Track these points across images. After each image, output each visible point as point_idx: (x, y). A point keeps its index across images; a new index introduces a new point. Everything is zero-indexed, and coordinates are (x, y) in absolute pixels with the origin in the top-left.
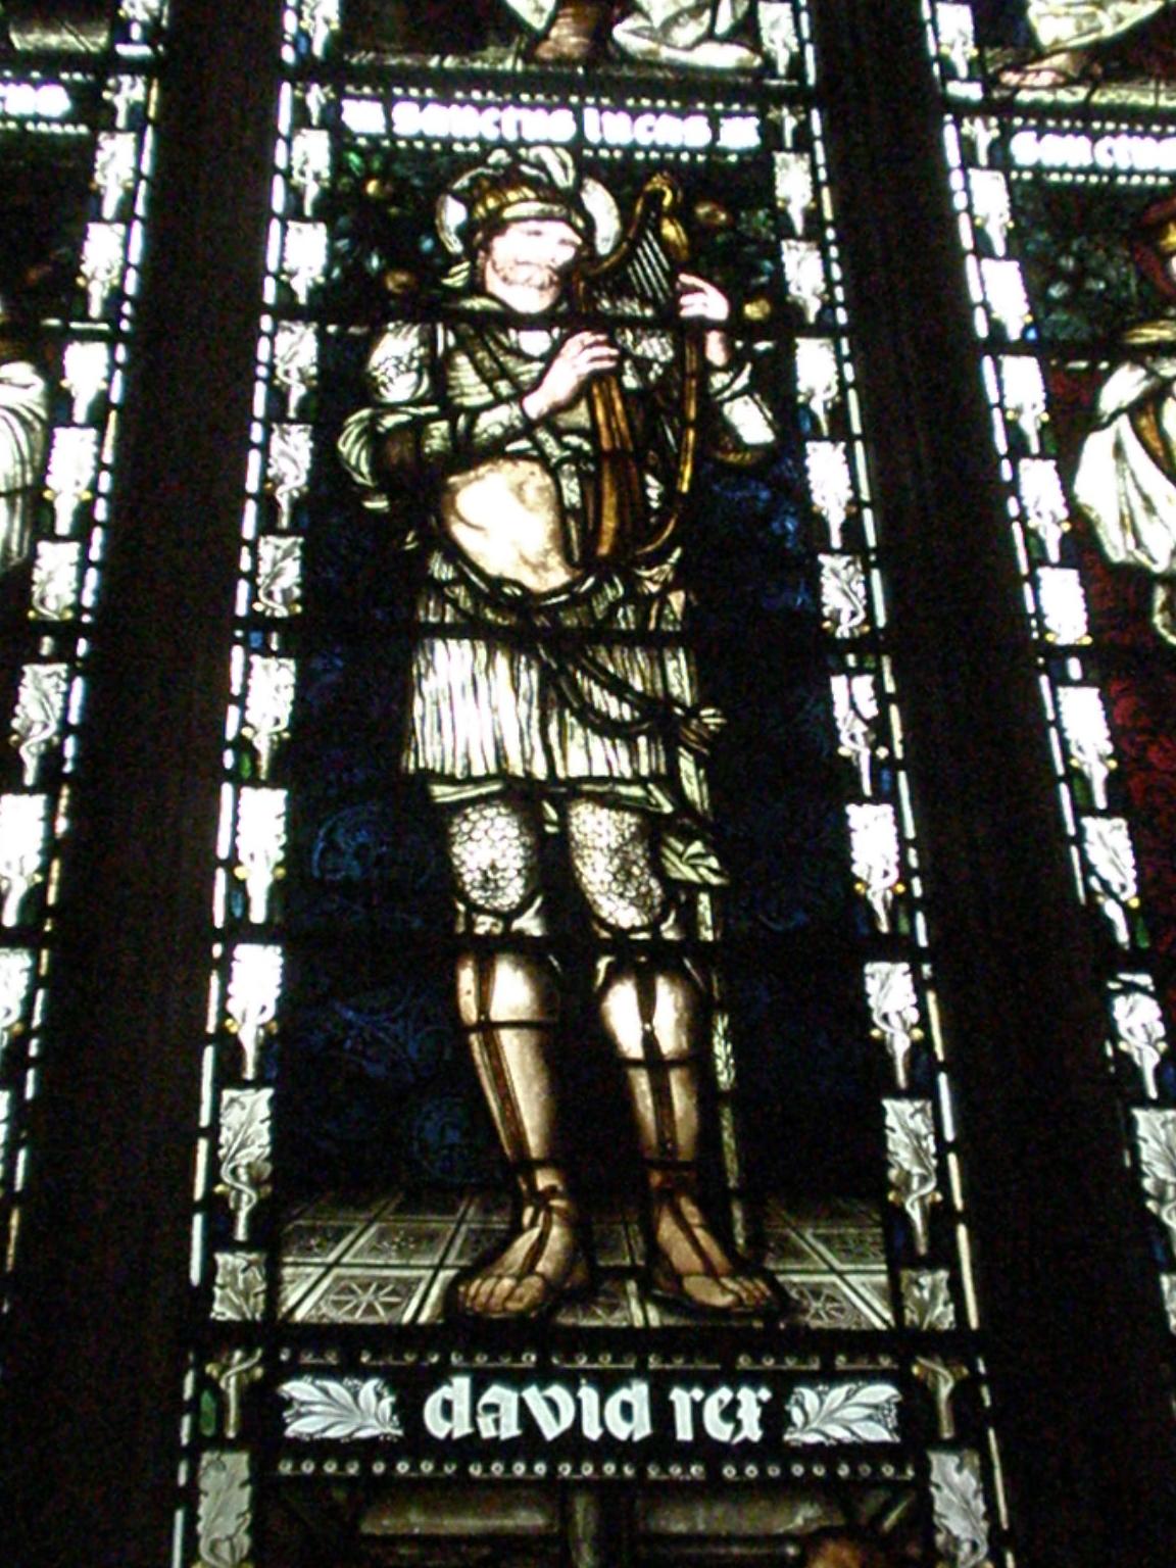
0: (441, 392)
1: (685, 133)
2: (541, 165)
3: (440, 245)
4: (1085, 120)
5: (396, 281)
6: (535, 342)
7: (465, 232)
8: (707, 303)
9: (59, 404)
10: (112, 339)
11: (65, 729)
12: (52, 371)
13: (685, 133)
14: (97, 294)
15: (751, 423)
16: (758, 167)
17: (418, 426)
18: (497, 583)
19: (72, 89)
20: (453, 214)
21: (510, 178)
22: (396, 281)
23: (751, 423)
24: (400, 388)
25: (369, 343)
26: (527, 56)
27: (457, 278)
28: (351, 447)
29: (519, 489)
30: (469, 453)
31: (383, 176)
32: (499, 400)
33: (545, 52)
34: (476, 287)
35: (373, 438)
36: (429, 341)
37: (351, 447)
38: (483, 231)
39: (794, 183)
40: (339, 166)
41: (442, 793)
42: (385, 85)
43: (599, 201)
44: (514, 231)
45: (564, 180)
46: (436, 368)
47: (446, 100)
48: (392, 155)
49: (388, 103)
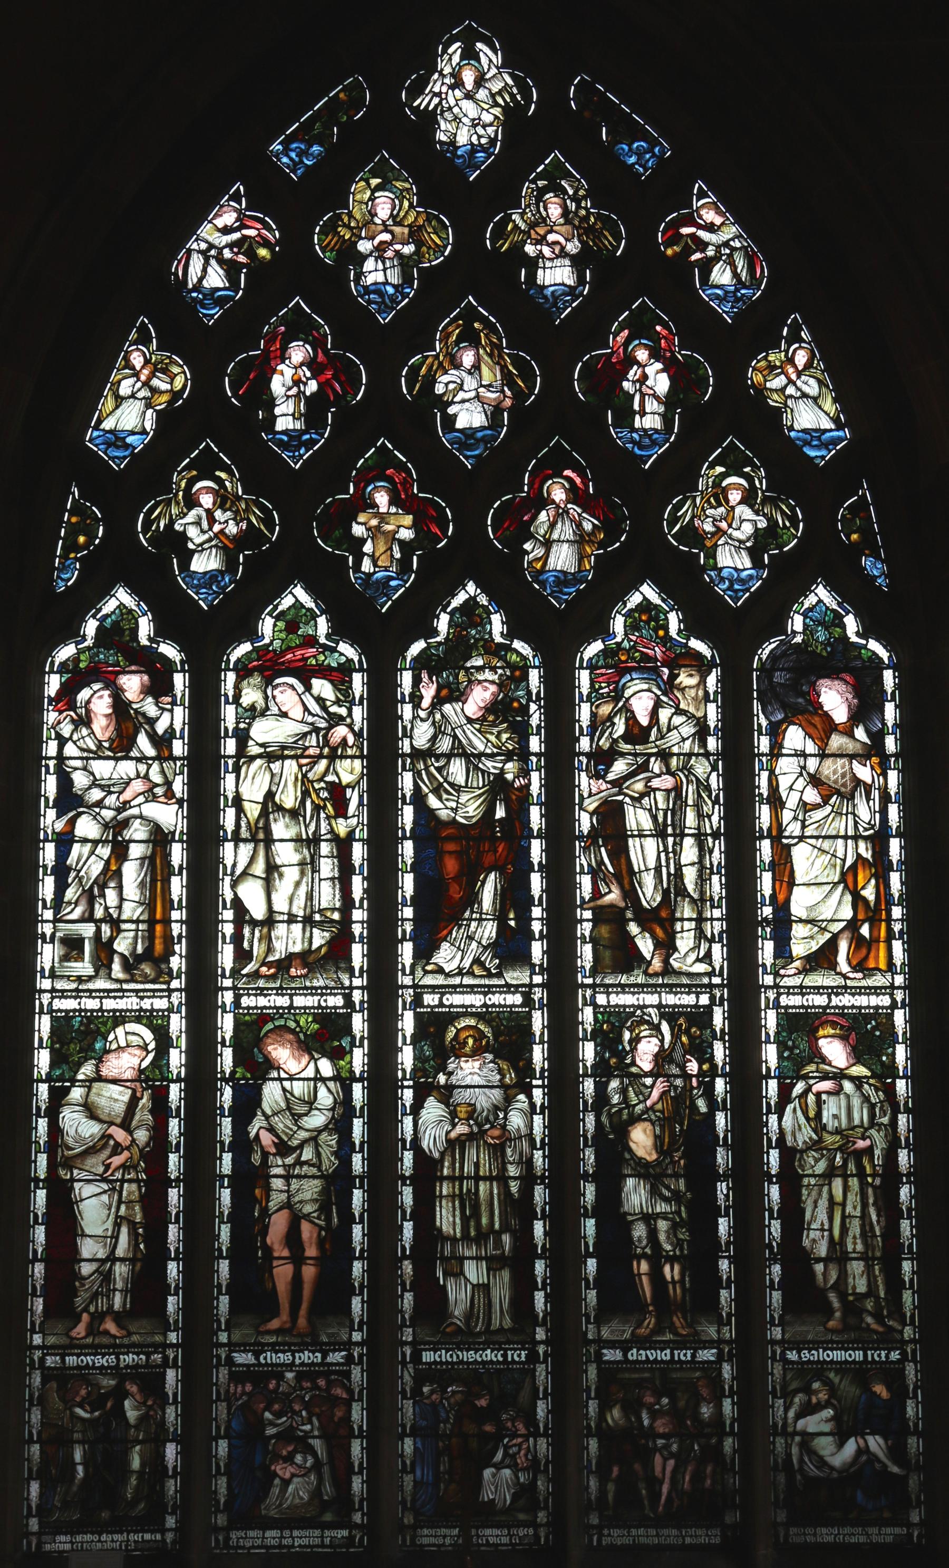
0: (625, 1099)
1: (689, 1000)
2: (650, 1015)
3: (624, 1048)
4: (802, 990)
5: (613, 1061)
6: (648, 1081)
7: (630, 1042)
8: (693, 1067)
9: (532, 1105)
10: (543, 1086)
11: (545, 1203)
12: (530, 1096)
13: (689, 1000)
14: (538, 1070)
15: (702, 1105)
16: (709, 1010)
17: (621, 1110)
18: (641, 1159)
19: (522, 993)
20: (627, 1035)
21: (642, 1022)
22: (613, 1061)
23: (702, 1105)
24: (616, 1099)
25: (607, 1083)
26: (646, 973)
27: (628, 1061)
28: (604, 1119)
29: (645, 1131)
30: (635, 1119)
31: (608, 1022)
32: (640, 1102)
33: (650, 971)
34: (633, 1063)
35: (610, 1116)
36: (622, 1083)
37: (604, 1119)
38: (636, 1040)
39: (718, 1018)
40: (596, 1019)
41: (630, 1218)
42: (607, 989)
43: (665, 1027)
44: (644, 1041)
45: (656, 1021)
46: (623, 1091)
47: (624, 992)
48: (610, 1013)
49: (608, 994)
